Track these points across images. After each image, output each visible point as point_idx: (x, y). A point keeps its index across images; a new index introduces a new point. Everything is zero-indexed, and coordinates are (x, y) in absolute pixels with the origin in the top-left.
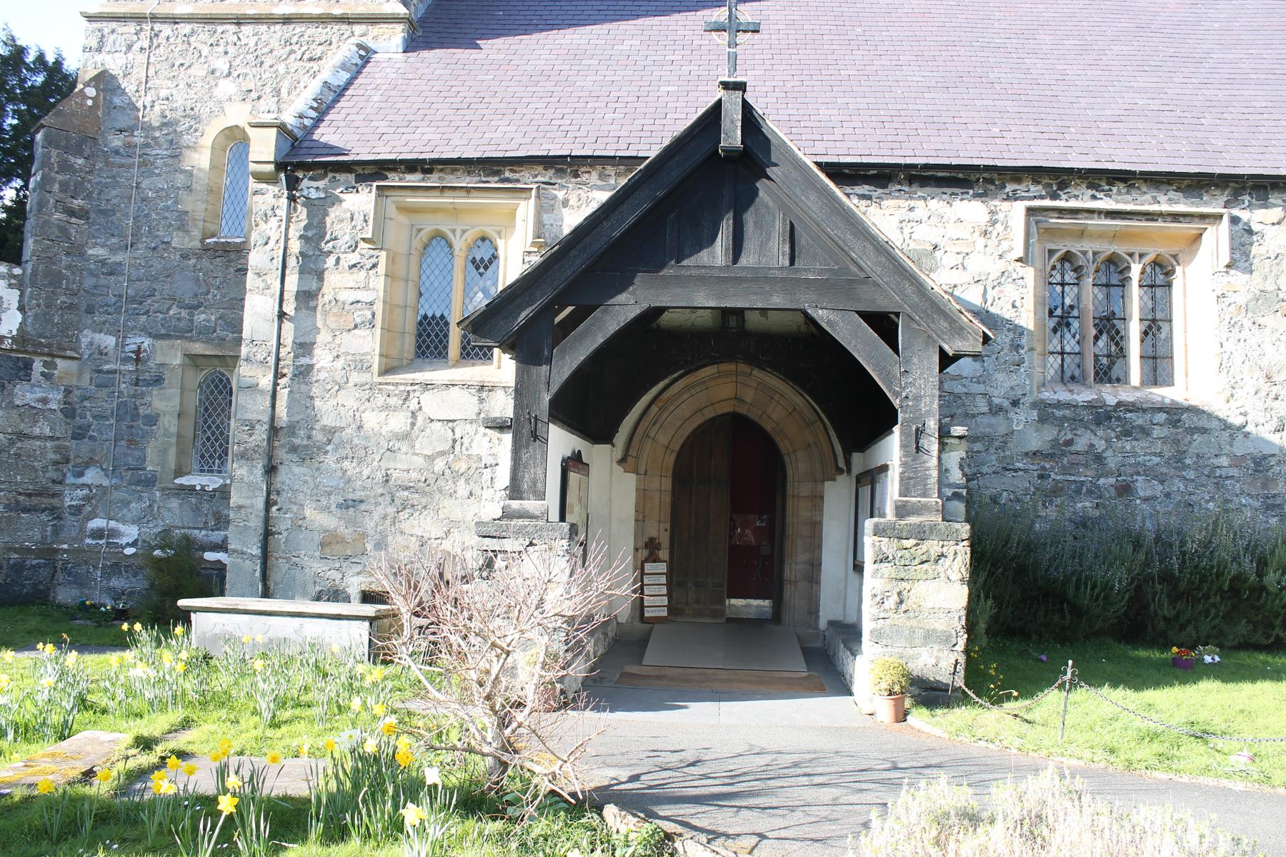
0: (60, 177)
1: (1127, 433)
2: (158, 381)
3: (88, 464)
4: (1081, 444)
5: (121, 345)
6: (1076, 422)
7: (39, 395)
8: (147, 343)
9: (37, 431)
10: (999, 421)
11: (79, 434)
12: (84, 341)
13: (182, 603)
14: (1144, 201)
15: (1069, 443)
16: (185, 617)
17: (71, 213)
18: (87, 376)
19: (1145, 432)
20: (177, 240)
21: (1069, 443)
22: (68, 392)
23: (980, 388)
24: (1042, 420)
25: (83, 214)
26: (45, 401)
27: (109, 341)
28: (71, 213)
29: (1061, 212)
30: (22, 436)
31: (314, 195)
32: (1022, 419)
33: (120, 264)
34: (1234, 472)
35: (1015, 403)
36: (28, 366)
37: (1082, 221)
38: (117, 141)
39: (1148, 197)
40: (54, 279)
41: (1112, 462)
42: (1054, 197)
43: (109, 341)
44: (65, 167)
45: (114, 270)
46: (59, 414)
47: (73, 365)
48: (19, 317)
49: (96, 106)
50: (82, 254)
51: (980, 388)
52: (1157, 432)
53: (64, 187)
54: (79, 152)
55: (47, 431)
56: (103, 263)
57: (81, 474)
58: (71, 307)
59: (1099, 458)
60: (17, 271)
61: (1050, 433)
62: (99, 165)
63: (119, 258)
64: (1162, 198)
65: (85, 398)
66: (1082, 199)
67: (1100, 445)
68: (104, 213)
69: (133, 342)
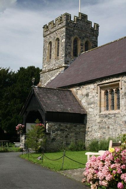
1: (109, 118)
10: (95, 118)
13: (14, 143)
14: (111, 80)
15: (102, 121)
16: (14, 144)
19: (111, 118)
21: (102, 121)
23: (93, 113)
32: (98, 117)
34: (122, 124)
41: (107, 123)
42: (101, 82)
52: (113, 118)
59: (106, 123)
61: (100, 119)
67: (106, 120)
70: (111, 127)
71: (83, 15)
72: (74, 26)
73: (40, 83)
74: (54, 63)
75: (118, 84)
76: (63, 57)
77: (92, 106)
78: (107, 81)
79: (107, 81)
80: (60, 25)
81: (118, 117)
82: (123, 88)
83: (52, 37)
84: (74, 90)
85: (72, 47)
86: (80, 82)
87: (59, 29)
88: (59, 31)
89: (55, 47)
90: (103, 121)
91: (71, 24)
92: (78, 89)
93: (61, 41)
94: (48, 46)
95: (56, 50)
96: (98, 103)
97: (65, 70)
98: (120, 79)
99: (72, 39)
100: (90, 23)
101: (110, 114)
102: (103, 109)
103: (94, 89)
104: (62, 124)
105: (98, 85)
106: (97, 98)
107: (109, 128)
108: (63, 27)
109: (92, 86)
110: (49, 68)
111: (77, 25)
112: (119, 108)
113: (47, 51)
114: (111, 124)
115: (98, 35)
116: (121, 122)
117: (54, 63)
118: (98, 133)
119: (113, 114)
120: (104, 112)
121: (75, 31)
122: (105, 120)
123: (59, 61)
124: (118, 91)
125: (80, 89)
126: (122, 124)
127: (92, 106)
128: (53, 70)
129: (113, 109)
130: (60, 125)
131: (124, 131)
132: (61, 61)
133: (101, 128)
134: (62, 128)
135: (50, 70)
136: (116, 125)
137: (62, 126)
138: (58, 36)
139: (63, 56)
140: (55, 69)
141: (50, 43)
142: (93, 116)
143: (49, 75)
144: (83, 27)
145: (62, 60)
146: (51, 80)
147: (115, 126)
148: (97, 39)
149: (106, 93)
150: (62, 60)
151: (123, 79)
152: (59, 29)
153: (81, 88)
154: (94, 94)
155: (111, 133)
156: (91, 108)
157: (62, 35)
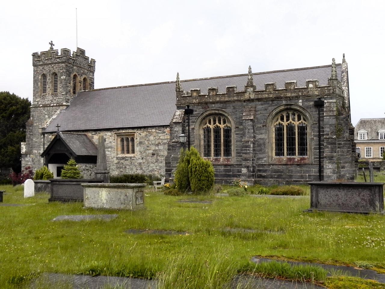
0: (29, 130)
3: (35, 168)
4: (121, 162)
5: (38, 152)
6: (120, 159)
7: (29, 159)
9: (29, 164)
10: (112, 159)
11: (34, 164)
12: (34, 151)
14: (127, 131)
15: (120, 162)
17: (31, 135)
18: (34, 156)
21: (120, 162)
22: (32, 158)
23: (110, 156)
24: (117, 159)
25: (32, 135)
26: (29, 160)
27: (36, 151)
28: (31, 135)
29: (119, 133)
30: (27, 164)
31: (46, 136)
32: (115, 159)
33: (37, 141)
34: (137, 165)
35: (114, 157)
36: (27, 156)
37: (120, 134)
38: (35, 124)
39: (128, 130)
40: (29, 144)
41: (124, 164)
42: (118, 131)
43: (36, 151)
44: (29, 129)
45: (36, 142)
46: (32, 162)
47: (33, 155)
48: (25, 149)
49: (32, 120)
50: (33, 140)
51: (110, 156)
52: (129, 160)
53: (29, 132)
54: (31, 127)
55: (30, 164)
56: (35, 141)
57: (34, 169)
58: (32, 147)
59: (123, 164)
60: (25, 143)
61: (118, 161)
62: (34, 128)
63: (37, 140)
64: (130, 130)
65: (34, 159)
66: (121, 131)
67: (123, 162)
70: (127, 167)
71: (81, 51)
72: (74, 63)
73: (31, 118)
74: (51, 98)
75: (134, 135)
76: (62, 95)
77: (109, 149)
78: (124, 131)
79: (124, 131)
80: (58, 60)
81: (134, 160)
82: (138, 138)
83: (47, 69)
84: (89, 134)
85: (72, 84)
86: (96, 128)
87: (56, 63)
88: (57, 66)
89: (52, 81)
90: (121, 162)
91: (71, 60)
92: (93, 134)
93: (60, 77)
94: (40, 78)
95: (52, 85)
96: (115, 147)
97: (66, 108)
98: (135, 131)
99: (72, 76)
100: (87, 59)
101: (126, 157)
102: (119, 152)
103: (111, 136)
104: (87, 165)
105: (115, 133)
106: (114, 144)
107: (125, 167)
108: (63, 62)
109: (109, 133)
110: (44, 103)
111: (76, 61)
112: (133, 152)
113: (39, 84)
114: (127, 165)
115: (95, 71)
116: (136, 163)
117: (51, 98)
118: (116, 172)
119: (129, 157)
120: (120, 155)
121: (75, 67)
122: (122, 161)
123: (57, 98)
124: (133, 140)
125: (96, 134)
126: (137, 165)
127: (109, 150)
128: (50, 106)
129: (128, 152)
130: (86, 166)
131: (139, 170)
132: (61, 98)
133: (118, 168)
134: (87, 168)
135: (45, 106)
136: (132, 165)
137: (87, 167)
138: (57, 71)
139: (63, 93)
141: (44, 76)
142: (111, 158)
143: (44, 111)
144: (81, 63)
145: (62, 97)
146: (53, 119)
147: (131, 166)
148: (93, 75)
149: (122, 140)
150: (62, 97)
151: (137, 131)
153: (97, 133)
154: (111, 140)
155: (127, 171)
156: (109, 151)
157: (61, 71)
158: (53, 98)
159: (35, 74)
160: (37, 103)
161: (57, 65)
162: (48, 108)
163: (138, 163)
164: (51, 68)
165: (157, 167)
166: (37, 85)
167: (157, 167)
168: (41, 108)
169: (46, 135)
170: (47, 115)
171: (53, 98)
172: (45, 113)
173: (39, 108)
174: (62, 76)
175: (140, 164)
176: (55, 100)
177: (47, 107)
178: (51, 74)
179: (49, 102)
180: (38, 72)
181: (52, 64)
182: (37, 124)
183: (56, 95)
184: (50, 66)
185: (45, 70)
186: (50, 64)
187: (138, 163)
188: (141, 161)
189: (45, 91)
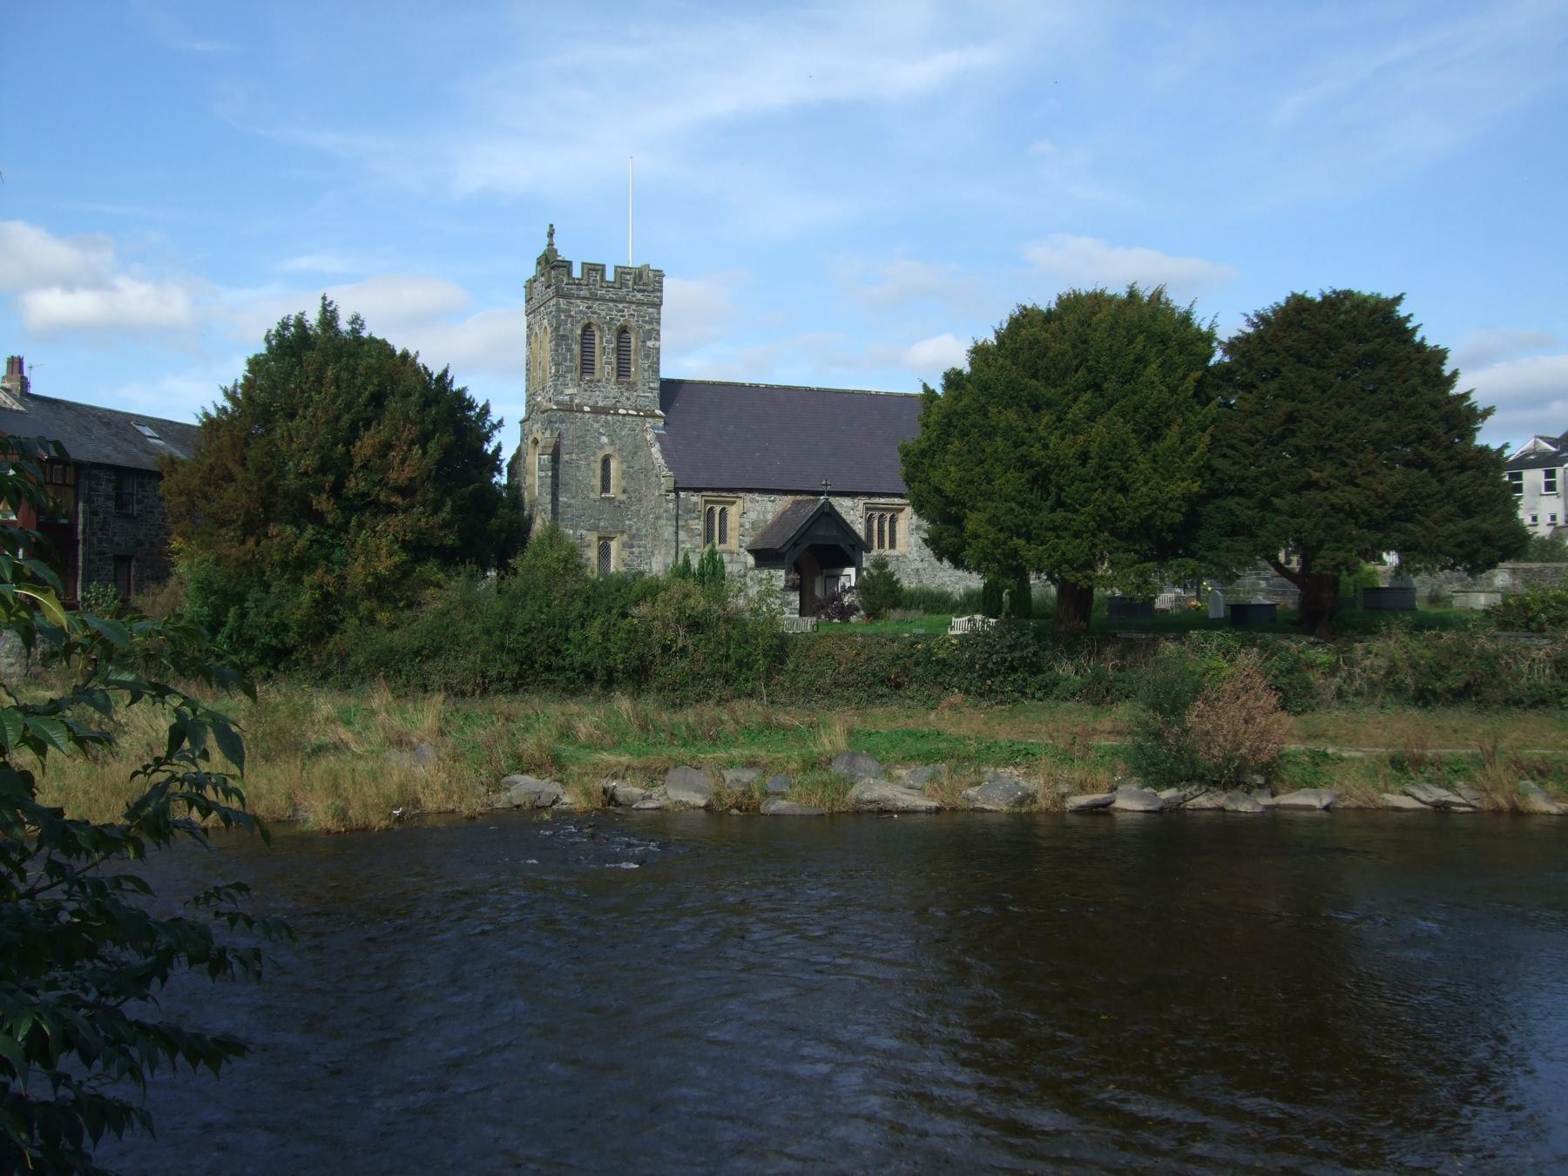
2: (589, 546)
8: (584, 532)
20: (592, 496)
45: (570, 506)
66: (877, 500)
68: (566, 485)
69: (579, 532)
76: (650, 388)
78: (882, 500)
80: (639, 296)
87: (633, 303)
93: (644, 342)
112: (893, 545)
124: (893, 521)
132: (647, 397)
135: (597, 411)
138: (633, 322)
139: (652, 385)
140: (624, 415)
143: (595, 425)
145: (650, 395)
150: (650, 395)
152: (633, 303)
158: (622, 393)
159: (563, 317)
160: (567, 398)
161: (634, 307)
162: (609, 418)
163: (912, 570)
164: (614, 312)
165: (952, 579)
166: (569, 350)
167: (952, 579)
168: (588, 416)
169: (682, 495)
170: (604, 435)
171: (622, 393)
172: (601, 430)
173: (579, 415)
174: (650, 339)
175: (917, 570)
176: (628, 399)
177: (608, 414)
178: (614, 327)
179: (609, 403)
180: (572, 313)
181: (621, 302)
182: (574, 457)
183: (631, 387)
184: (611, 304)
185: (593, 313)
186: (611, 300)
187: (912, 570)
188: (919, 565)
189: (587, 366)
